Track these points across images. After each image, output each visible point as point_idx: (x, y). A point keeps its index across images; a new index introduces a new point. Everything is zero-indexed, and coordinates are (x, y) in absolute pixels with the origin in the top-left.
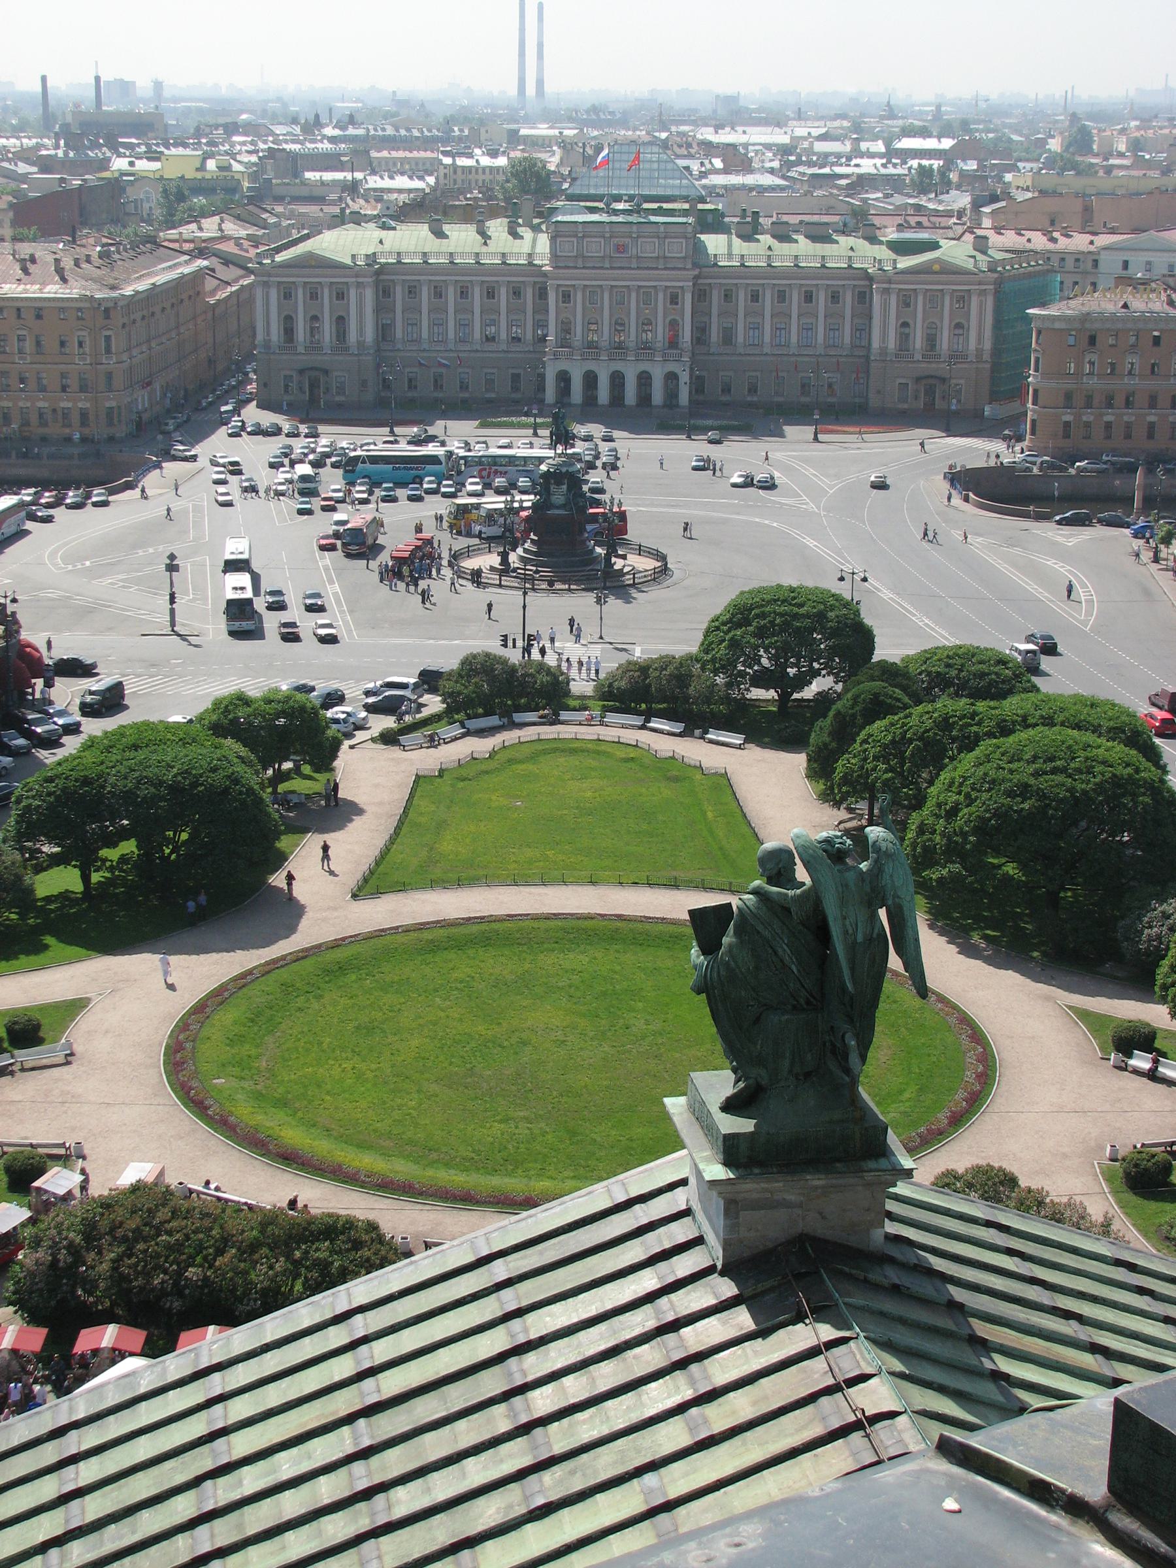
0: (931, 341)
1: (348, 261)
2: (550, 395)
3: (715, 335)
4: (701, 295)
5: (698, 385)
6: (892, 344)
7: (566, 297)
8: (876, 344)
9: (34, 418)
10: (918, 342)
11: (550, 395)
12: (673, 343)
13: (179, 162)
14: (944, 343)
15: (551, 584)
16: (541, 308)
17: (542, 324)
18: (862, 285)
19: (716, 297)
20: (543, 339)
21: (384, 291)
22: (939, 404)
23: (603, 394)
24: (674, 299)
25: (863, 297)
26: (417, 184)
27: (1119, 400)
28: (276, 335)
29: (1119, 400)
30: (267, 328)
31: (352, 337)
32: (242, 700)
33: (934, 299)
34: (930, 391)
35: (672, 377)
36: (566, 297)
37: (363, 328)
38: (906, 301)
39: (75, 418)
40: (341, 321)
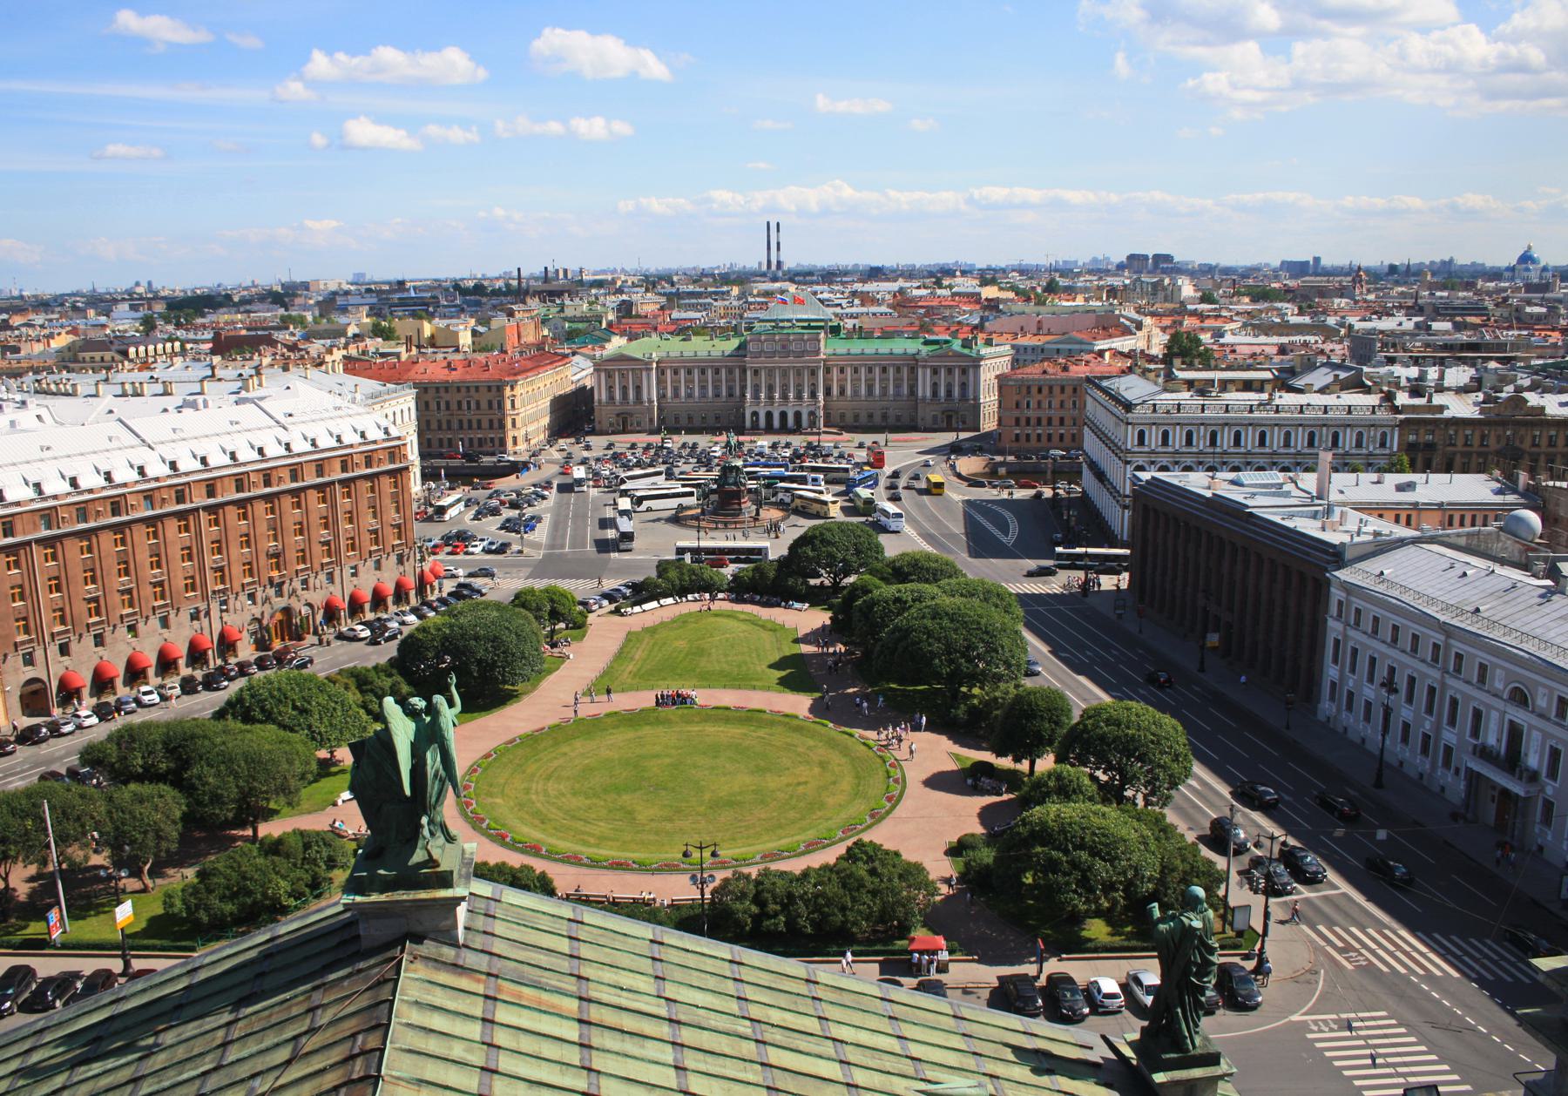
0: (949, 393)
1: (639, 356)
2: (748, 424)
3: (835, 391)
4: (828, 370)
5: (827, 416)
6: (928, 394)
7: (756, 372)
8: (920, 394)
9: (476, 443)
10: (942, 392)
11: (748, 424)
12: (813, 395)
13: (578, 307)
14: (956, 392)
15: (726, 524)
16: (743, 380)
17: (743, 388)
18: (913, 363)
19: (835, 372)
20: (744, 396)
21: (661, 372)
22: (954, 425)
23: (776, 423)
24: (813, 373)
25: (913, 370)
26: (698, 315)
27: (1044, 422)
28: (604, 397)
29: (1044, 422)
30: (601, 395)
31: (645, 397)
32: (532, 591)
33: (950, 371)
34: (949, 418)
35: (812, 414)
36: (756, 372)
37: (652, 392)
38: (935, 371)
39: (497, 442)
40: (638, 389)
